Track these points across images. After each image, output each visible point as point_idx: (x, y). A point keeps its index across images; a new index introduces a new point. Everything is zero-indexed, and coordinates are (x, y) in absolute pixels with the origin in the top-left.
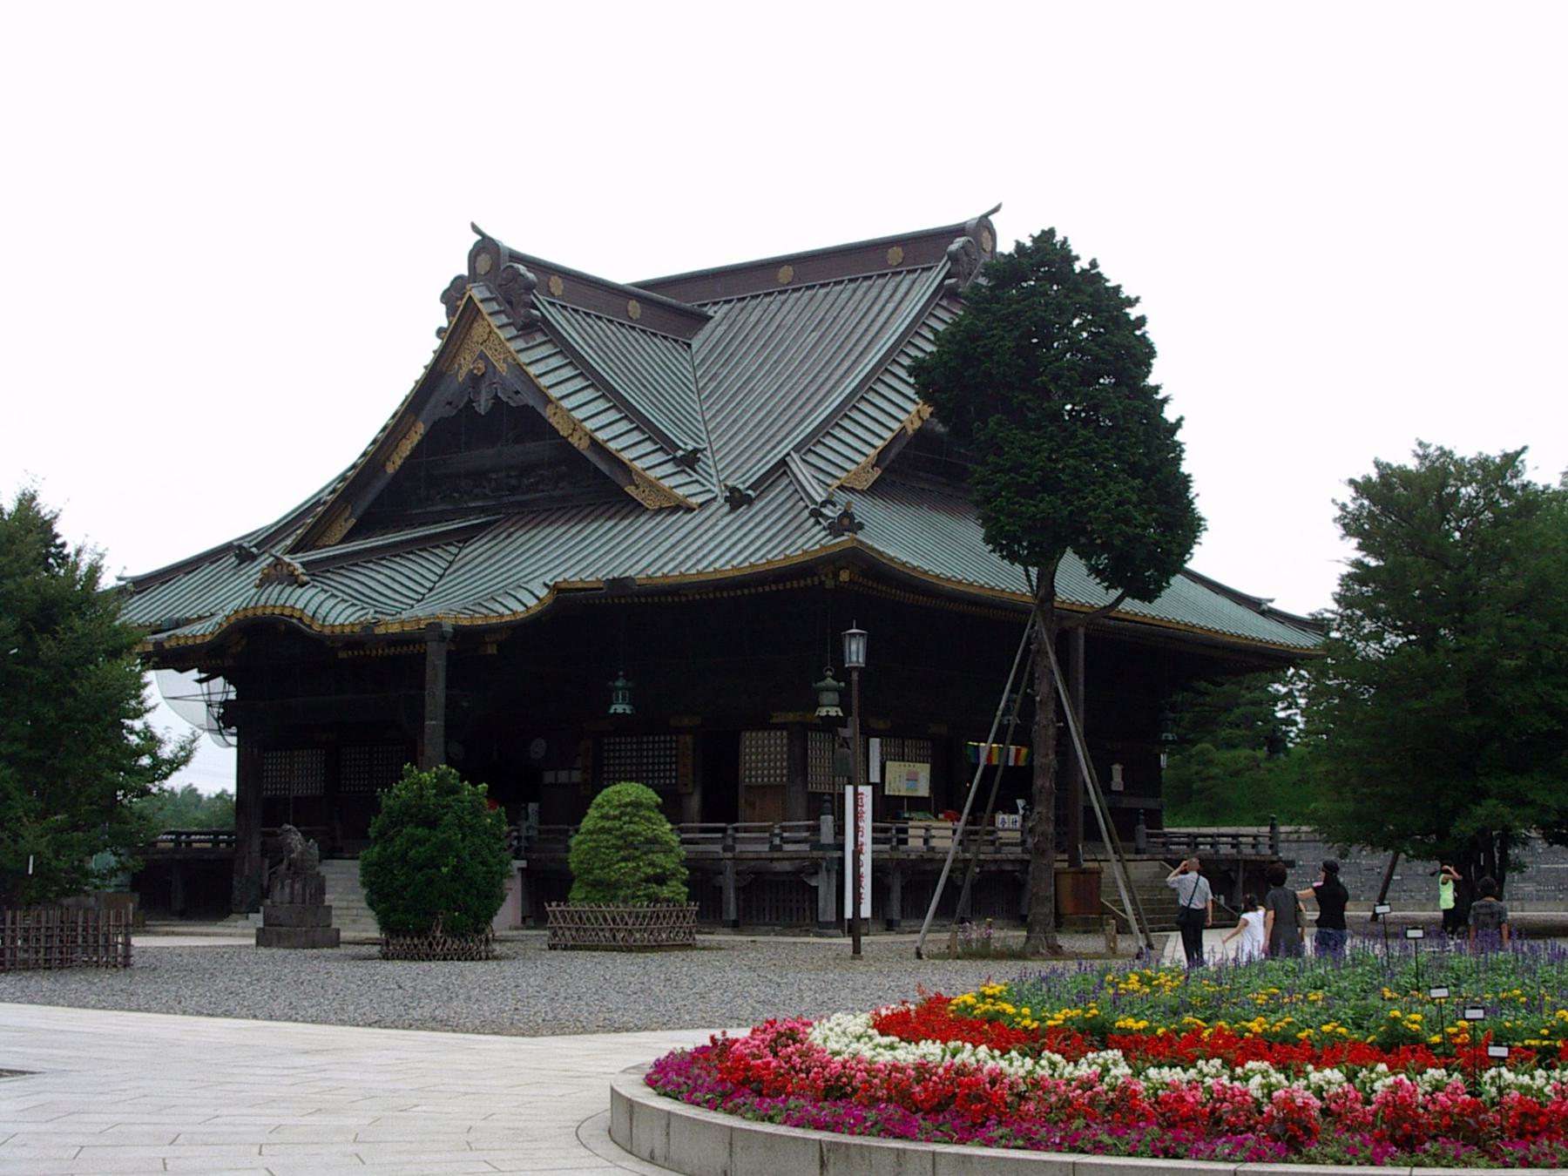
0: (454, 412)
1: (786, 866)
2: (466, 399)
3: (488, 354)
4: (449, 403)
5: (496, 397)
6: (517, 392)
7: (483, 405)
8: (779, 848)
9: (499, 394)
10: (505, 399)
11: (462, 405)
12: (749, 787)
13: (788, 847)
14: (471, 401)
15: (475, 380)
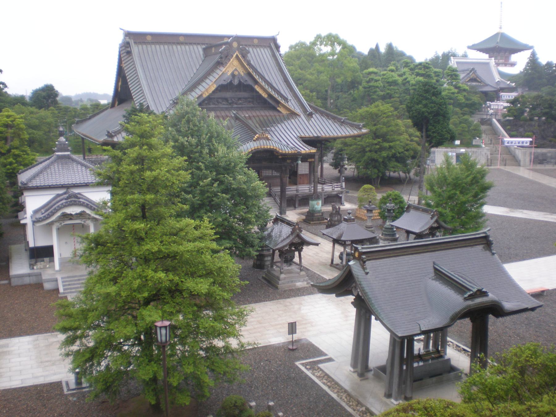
0: (226, 83)
1: (335, 193)
2: (230, 80)
3: (238, 69)
4: (225, 81)
5: (240, 81)
6: (246, 81)
7: (236, 82)
8: (334, 189)
9: (241, 80)
10: (243, 82)
11: (229, 82)
12: (300, 175)
13: (336, 189)
14: (231, 81)
15: (233, 75)
